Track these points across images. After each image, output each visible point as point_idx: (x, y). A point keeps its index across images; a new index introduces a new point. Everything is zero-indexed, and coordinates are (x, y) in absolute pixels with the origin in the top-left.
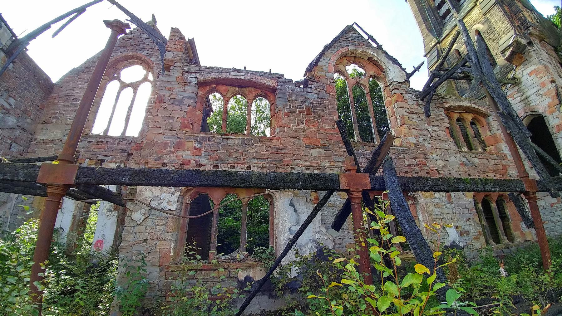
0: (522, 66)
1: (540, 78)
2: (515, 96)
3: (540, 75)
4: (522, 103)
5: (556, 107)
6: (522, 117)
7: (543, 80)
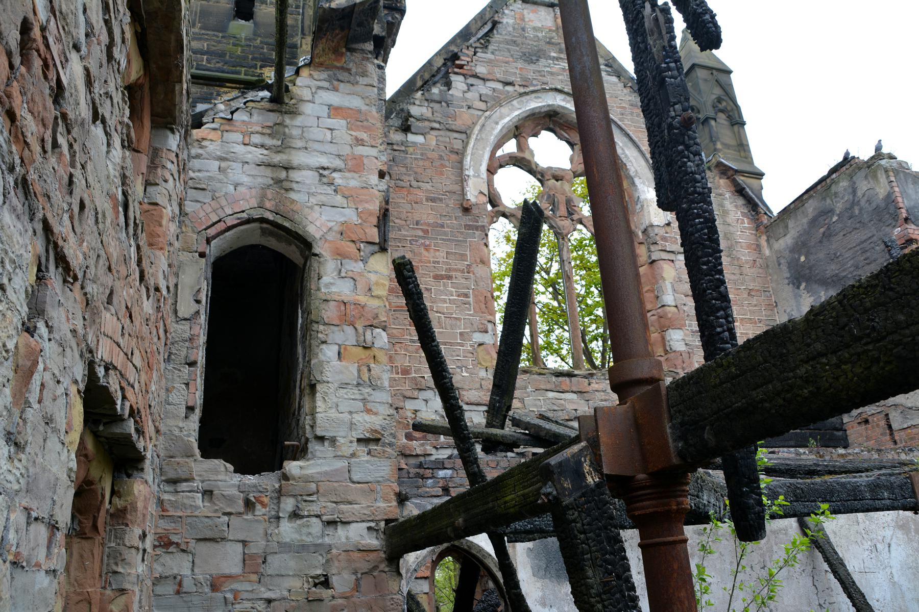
0: (324, 75)
1: (357, 139)
2: (256, 139)
3: (364, 136)
4: (268, 172)
5: (362, 245)
6: (244, 215)
7: (360, 150)
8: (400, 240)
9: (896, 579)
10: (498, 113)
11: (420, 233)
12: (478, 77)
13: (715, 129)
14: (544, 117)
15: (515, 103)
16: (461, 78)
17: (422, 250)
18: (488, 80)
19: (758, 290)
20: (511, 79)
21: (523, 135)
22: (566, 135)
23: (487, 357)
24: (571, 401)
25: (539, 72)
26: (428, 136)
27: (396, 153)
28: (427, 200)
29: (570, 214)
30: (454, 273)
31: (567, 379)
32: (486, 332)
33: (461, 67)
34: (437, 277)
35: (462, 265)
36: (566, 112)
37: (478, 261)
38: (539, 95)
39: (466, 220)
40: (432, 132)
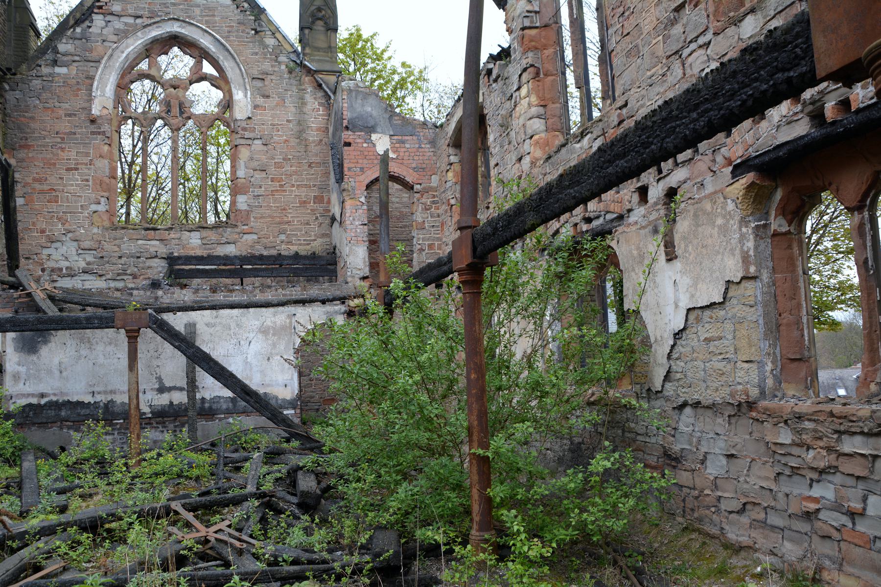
8: (44, 146)
9: (249, 360)
10: (124, 45)
11: (59, 140)
12: (114, 15)
13: (307, 36)
14: (169, 39)
15: (139, 34)
16: (101, 17)
17: (59, 151)
18: (121, 16)
19: (317, 163)
20: (140, 13)
21: (152, 55)
22: (189, 51)
23: (100, 220)
24: (153, 246)
25: (165, 4)
26: (71, 67)
27: (45, 83)
28: (65, 116)
29: (181, 113)
30: (79, 166)
31: (153, 232)
32: (100, 204)
33: (100, 7)
34: (68, 170)
35: (86, 160)
36: (182, 35)
37: (98, 156)
38: (160, 24)
39: (93, 128)
40: (75, 64)
